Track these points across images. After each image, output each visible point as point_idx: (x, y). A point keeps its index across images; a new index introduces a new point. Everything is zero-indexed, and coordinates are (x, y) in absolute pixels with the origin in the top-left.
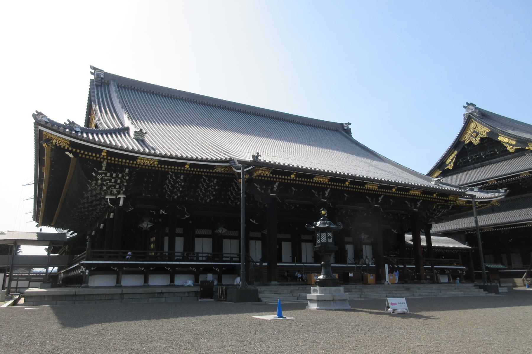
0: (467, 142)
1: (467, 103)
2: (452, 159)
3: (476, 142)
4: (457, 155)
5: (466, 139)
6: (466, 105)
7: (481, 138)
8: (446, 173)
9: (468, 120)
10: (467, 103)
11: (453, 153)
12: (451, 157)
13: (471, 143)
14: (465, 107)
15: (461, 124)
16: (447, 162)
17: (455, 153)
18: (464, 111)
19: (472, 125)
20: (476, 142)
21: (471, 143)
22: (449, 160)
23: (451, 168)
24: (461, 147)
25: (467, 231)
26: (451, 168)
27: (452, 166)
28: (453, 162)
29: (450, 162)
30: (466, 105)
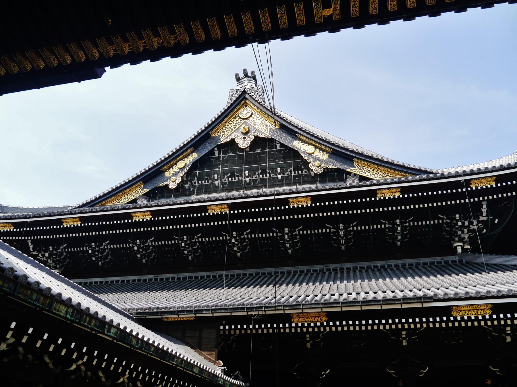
0: (223, 140)
1: (245, 71)
2: (182, 169)
3: (244, 143)
5: (225, 135)
6: (241, 75)
7: (256, 137)
9: (240, 100)
11: (186, 157)
12: (181, 164)
13: (232, 143)
14: (238, 79)
15: (223, 104)
16: (167, 174)
17: (194, 157)
19: (245, 112)
20: (244, 143)
21: (232, 143)
22: (175, 169)
23: (172, 186)
24: (209, 147)
25: (231, 320)
26: (172, 186)
29: (175, 174)
30: (241, 75)
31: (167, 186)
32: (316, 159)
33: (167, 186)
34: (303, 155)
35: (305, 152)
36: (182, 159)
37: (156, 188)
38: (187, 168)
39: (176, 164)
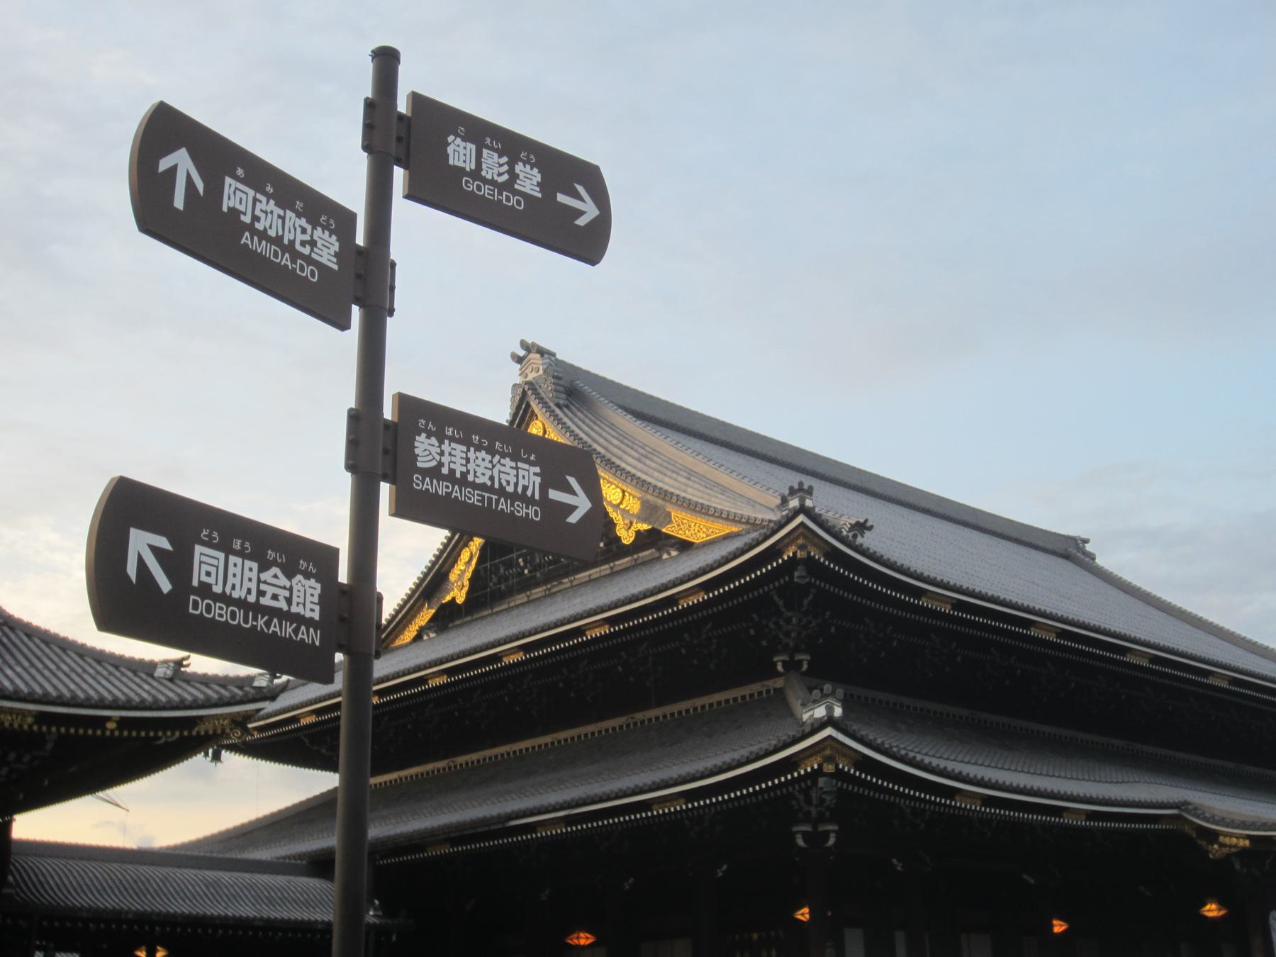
1: (524, 345)
4: (483, 550)
6: (522, 353)
8: (447, 618)
10: (524, 345)
12: (465, 555)
14: (519, 360)
16: (453, 577)
18: (513, 375)
22: (460, 566)
27: (466, 589)
28: (468, 575)
30: (522, 353)
31: (454, 599)
32: (625, 512)
33: (454, 599)
34: (609, 509)
35: (610, 503)
36: (466, 545)
37: (443, 607)
38: (474, 561)
39: (459, 555)
